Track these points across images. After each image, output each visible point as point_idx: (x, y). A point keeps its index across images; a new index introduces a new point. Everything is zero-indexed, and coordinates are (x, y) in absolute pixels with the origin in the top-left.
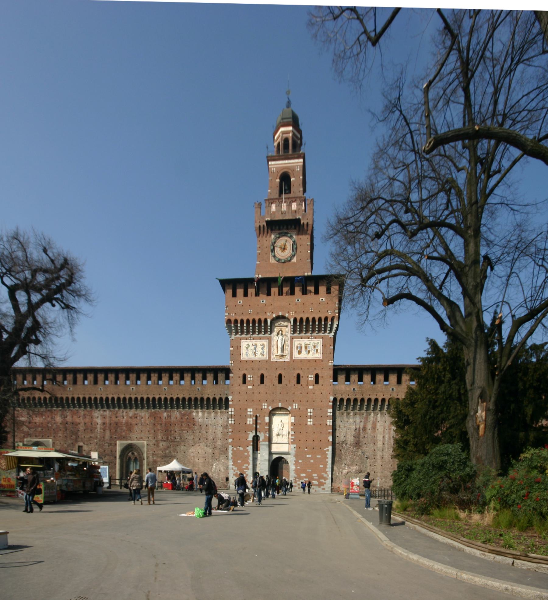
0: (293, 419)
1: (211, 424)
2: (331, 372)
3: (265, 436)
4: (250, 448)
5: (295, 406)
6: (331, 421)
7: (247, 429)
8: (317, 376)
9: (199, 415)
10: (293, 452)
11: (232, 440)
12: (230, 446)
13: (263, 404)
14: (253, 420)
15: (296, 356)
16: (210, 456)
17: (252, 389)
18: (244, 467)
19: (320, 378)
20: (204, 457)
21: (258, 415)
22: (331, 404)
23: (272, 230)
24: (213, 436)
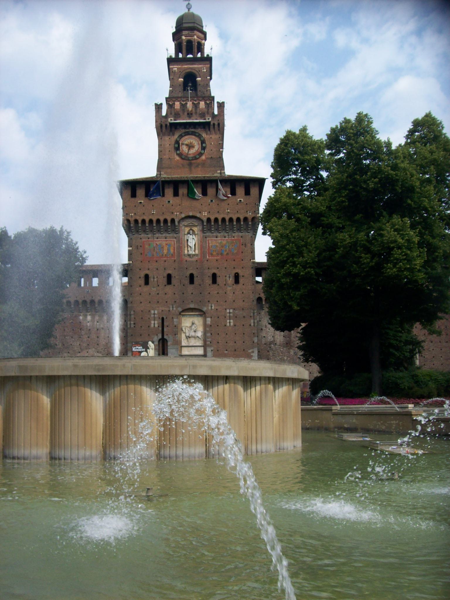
1: (103, 328)
6: (256, 321)
14: (158, 323)
19: (240, 277)
23: (176, 128)
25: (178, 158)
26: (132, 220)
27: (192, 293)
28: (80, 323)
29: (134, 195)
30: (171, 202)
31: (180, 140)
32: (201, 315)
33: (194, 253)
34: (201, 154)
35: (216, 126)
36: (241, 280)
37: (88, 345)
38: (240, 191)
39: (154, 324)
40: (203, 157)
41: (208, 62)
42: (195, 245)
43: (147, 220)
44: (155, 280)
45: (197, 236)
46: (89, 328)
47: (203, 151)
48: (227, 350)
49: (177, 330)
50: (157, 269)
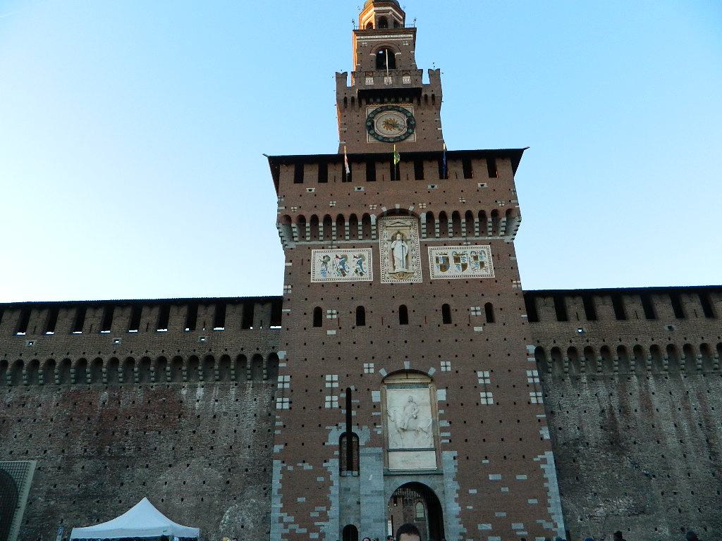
0: (442, 395)
1: (225, 414)
2: (522, 301)
3: (373, 435)
4: (333, 465)
5: (446, 366)
6: (540, 394)
7: (324, 419)
8: (489, 309)
9: (197, 395)
10: (450, 468)
11: (282, 447)
12: (275, 462)
13: (366, 365)
14: (339, 401)
15: (436, 273)
16: (218, 489)
17: (336, 336)
18: (312, 515)
20: (197, 494)
21: (353, 388)
22: (534, 359)
23: (368, 103)
24: (231, 440)
25: (370, 140)
26: (294, 217)
27: (406, 342)
28: (182, 402)
29: (299, 179)
30: (362, 189)
31: (373, 118)
32: (425, 385)
33: (405, 270)
34: (408, 135)
35: (430, 99)
36: (498, 315)
37: (191, 449)
38: (480, 169)
39: (332, 401)
40: (412, 139)
41: (412, 36)
42: (407, 256)
43: (321, 218)
44: (335, 317)
45: (409, 242)
46: (197, 414)
47: (410, 131)
48: (486, 458)
49: (377, 416)
50: (338, 298)
